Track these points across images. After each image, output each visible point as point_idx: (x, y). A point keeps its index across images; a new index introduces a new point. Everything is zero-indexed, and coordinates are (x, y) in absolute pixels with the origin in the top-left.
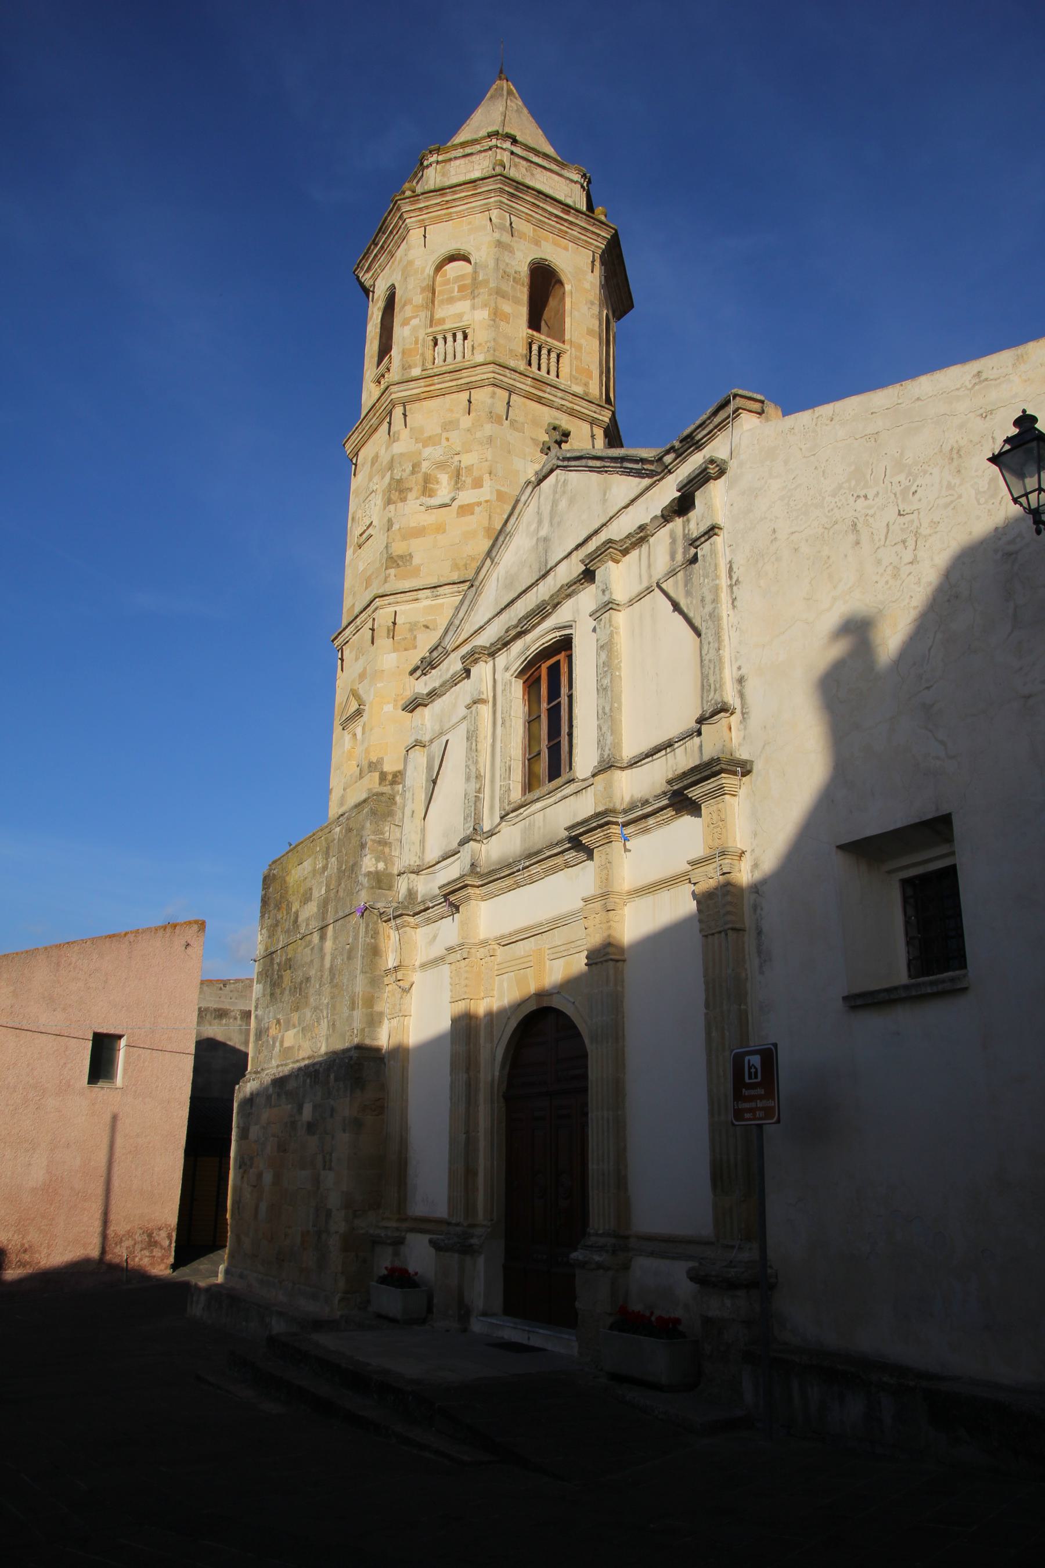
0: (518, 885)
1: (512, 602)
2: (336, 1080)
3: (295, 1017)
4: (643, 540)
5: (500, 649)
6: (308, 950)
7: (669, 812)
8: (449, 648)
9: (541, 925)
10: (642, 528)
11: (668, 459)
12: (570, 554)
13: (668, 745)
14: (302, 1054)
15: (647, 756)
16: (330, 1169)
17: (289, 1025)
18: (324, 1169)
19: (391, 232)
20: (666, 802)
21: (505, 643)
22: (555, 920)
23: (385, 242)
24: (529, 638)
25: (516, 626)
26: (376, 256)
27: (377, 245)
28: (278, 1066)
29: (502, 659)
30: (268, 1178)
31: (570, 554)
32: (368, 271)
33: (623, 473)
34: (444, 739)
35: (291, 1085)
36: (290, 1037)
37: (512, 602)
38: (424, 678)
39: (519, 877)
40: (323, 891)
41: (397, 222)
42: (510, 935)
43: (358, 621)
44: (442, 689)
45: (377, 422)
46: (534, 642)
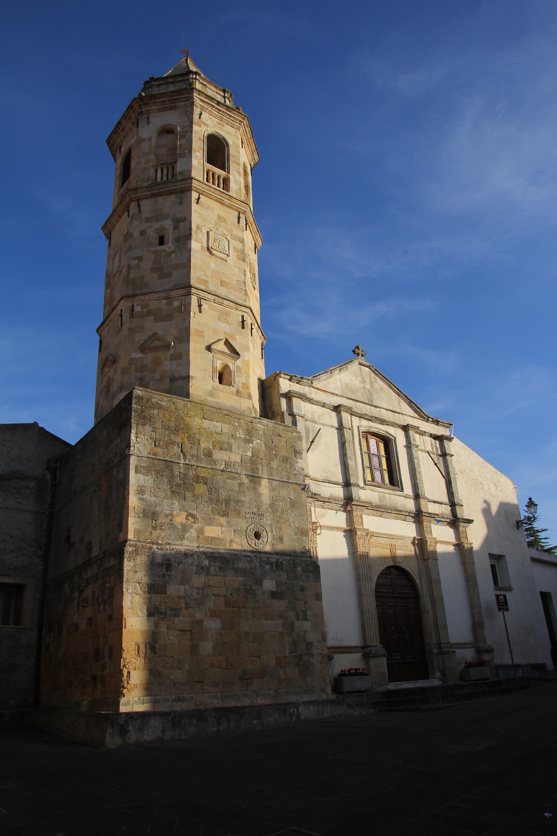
0: (381, 516)
1: (358, 401)
2: (304, 571)
3: (223, 520)
4: (422, 435)
5: (356, 416)
6: (236, 483)
7: (448, 524)
8: (313, 385)
9: (395, 536)
10: (425, 432)
11: (430, 419)
12: (388, 410)
13: (441, 503)
14: (235, 547)
15: (433, 502)
16: (306, 620)
17: (210, 522)
18: (298, 619)
19: (230, 116)
20: (448, 521)
21: (361, 416)
22: (401, 536)
23: (223, 112)
24: (371, 424)
25: (370, 417)
26: (213, 106)
27: (218, 105)
28: (198, 547)
29: (356, 420)
30: (213, 625)
31: (388, 410)
32: (201, 100)
33: (408, 404)
34: (318, 427)
35: (241, 565)
36: (211, 531)
37: (358, 401)
38: (288, 381)
39: (385, 514)
40: (249, 454)
41: (237, 120)
42: (380, 534)
43: (225, 302)
44: (315, 403)
45: (228, 204)
46: (375, 428)
